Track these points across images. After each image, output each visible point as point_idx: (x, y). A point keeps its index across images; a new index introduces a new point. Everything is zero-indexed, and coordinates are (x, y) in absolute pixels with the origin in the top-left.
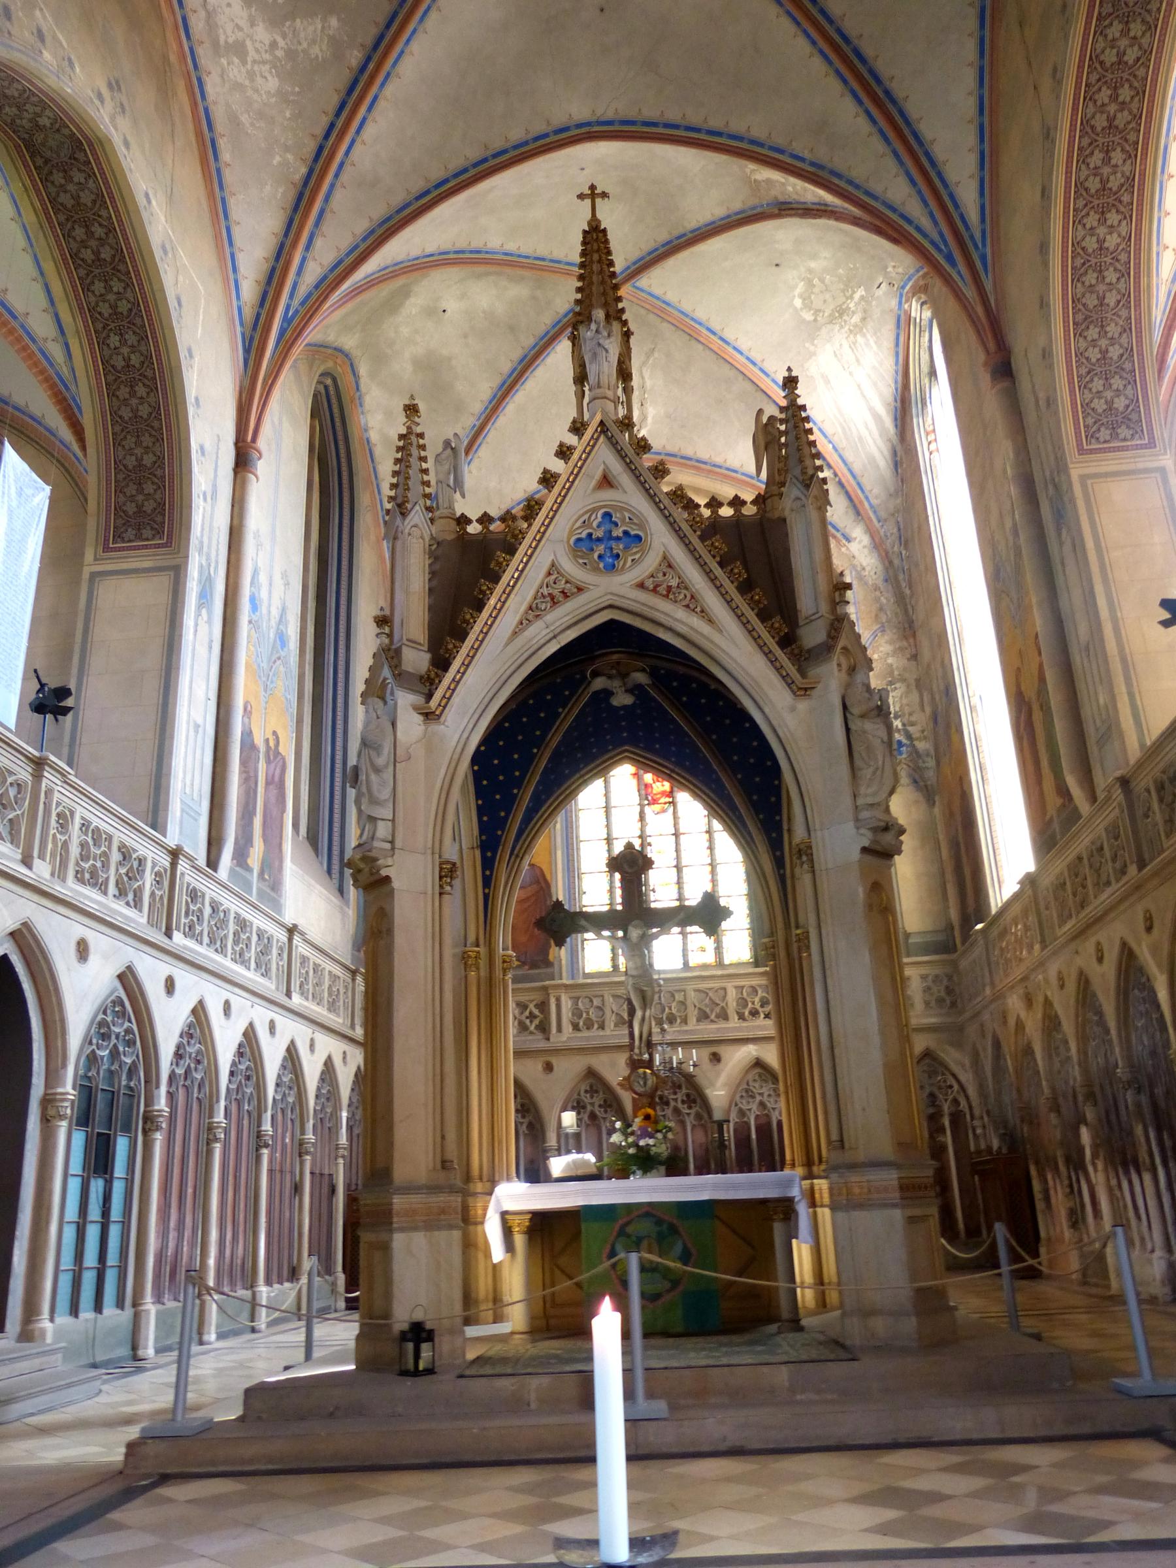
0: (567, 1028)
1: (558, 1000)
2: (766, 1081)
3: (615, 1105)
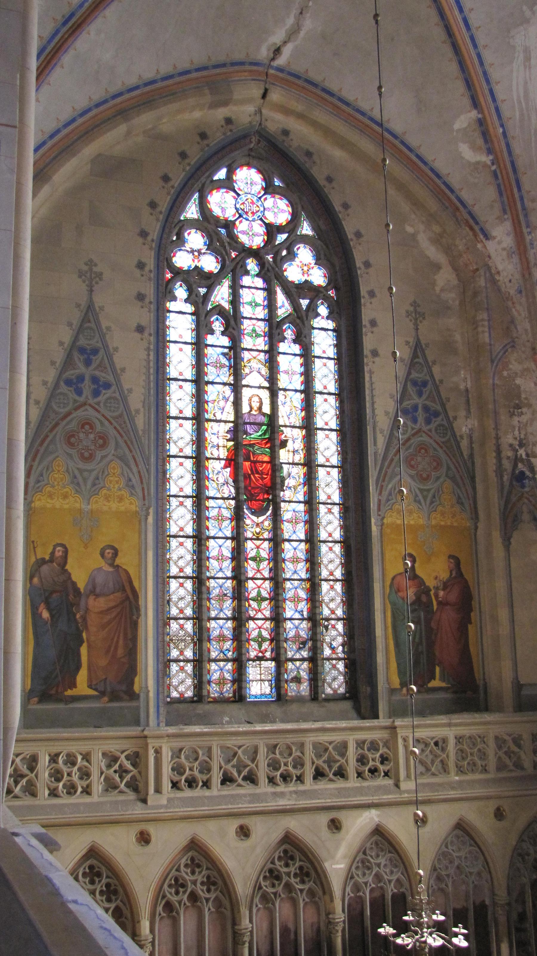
0: (166, 785)
1: (158, 752)
2: (382, 850)
3: (220, 882)
